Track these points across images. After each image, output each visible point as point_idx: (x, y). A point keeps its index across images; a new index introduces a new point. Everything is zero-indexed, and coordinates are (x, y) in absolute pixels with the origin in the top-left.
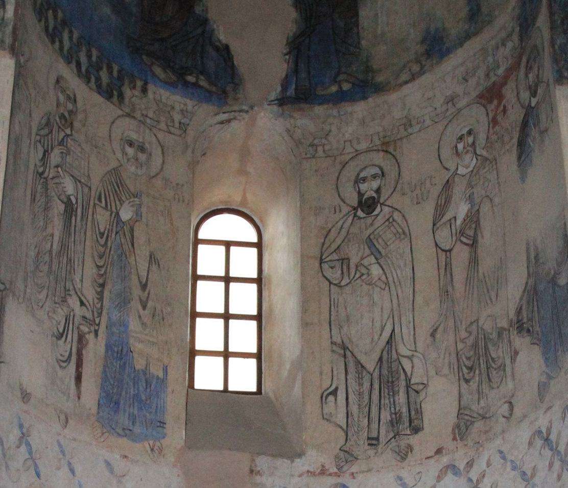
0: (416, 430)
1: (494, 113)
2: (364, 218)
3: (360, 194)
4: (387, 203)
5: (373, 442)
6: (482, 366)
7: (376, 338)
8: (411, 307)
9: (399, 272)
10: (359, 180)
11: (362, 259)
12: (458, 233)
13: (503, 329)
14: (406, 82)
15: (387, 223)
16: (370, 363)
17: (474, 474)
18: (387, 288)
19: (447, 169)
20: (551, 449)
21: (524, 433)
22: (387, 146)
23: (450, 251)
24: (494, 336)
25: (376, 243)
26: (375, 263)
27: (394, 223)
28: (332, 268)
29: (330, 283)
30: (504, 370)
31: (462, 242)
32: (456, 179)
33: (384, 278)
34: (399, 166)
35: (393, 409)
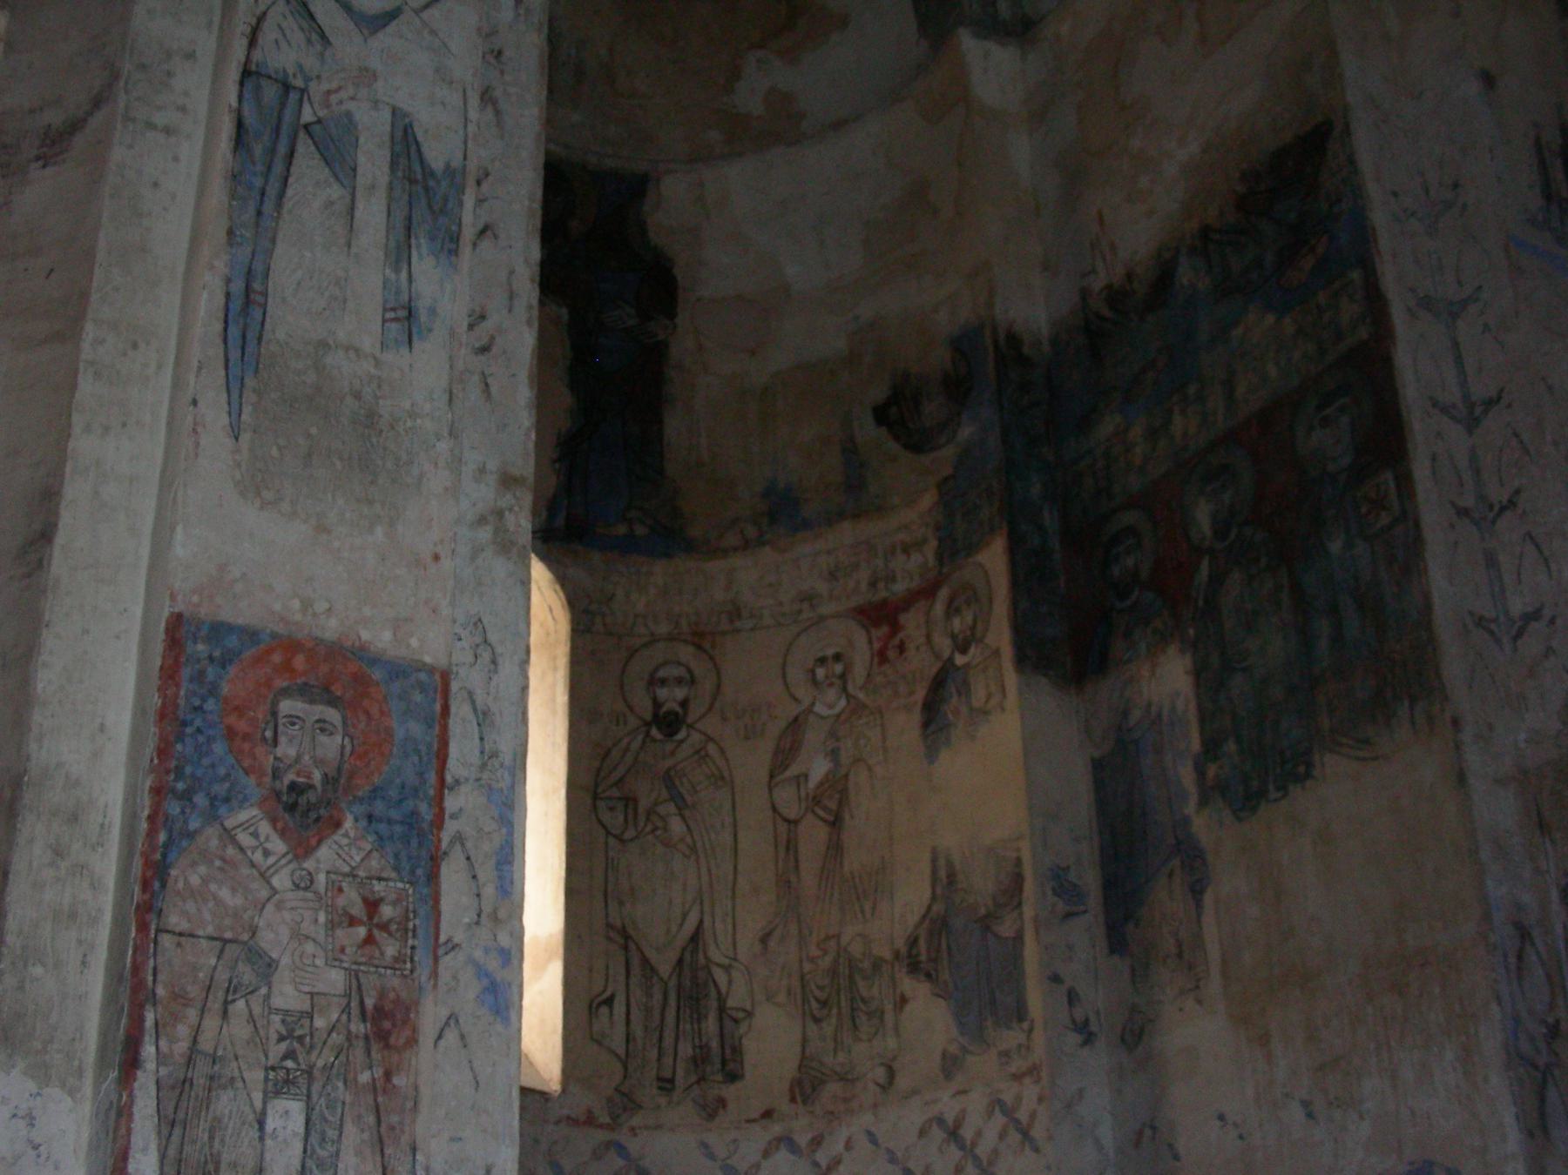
0: (733, 1077)
1: (882, 643)
2: (661, 741)
3: (657, 704)
4: (696, 726)
5: (666, 1084)
6: (843, 1004)
7: (674, 929)
8: (730, 894)
9: (713, 835)
10: (654, 681)
11: (656, 804)
12: (810, 799)
13: (882, 959)
14: (735, 549)
15: (696, 757)
16: (665, 968)
17: (822, 1157)
18: (693, 858)
19: (796, 700)
20: (962, 1147)
21: (913, 1116)
22: (701, 639)
23: (796, 822)
24: (866, 964)
25: (677, 783)
26: (676, 815)
27: (707, 759)
28: (611, 809)
29: (608, 833)
30: (882, 1020)
31: (813, 811)
32: (812, 718)
33: (689, 840)
34: (719, 674)
35: (697, 1040)
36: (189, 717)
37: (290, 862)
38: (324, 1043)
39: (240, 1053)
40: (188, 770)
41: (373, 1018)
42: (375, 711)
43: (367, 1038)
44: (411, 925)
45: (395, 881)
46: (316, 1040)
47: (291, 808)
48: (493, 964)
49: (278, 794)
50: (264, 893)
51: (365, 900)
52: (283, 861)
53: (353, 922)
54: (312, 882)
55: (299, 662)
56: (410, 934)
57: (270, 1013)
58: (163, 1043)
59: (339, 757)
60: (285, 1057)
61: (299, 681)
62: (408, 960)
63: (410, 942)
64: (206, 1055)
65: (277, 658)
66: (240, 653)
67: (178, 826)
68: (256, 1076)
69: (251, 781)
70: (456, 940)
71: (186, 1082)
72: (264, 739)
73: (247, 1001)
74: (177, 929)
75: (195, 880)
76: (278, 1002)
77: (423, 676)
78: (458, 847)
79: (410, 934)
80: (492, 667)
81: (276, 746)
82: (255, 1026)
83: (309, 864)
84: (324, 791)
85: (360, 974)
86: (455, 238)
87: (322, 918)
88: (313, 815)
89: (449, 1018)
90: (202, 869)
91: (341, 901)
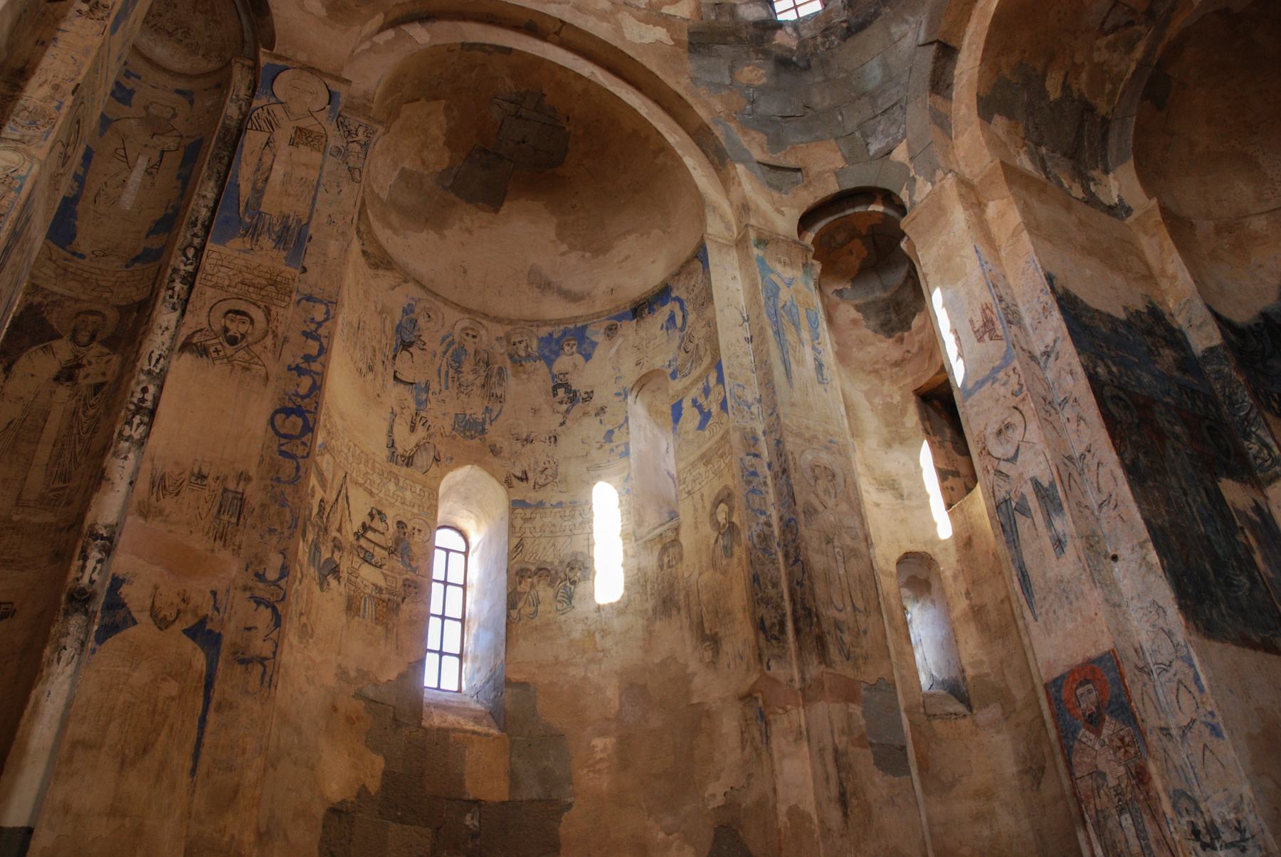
48: (1209, 719)
53: (1119, 748)
65: (1071, 679)
68: (1114, 811)
71: (1098, 821)
76: (1110, 785)
86: (1061, 505)
91: (1114, 744)
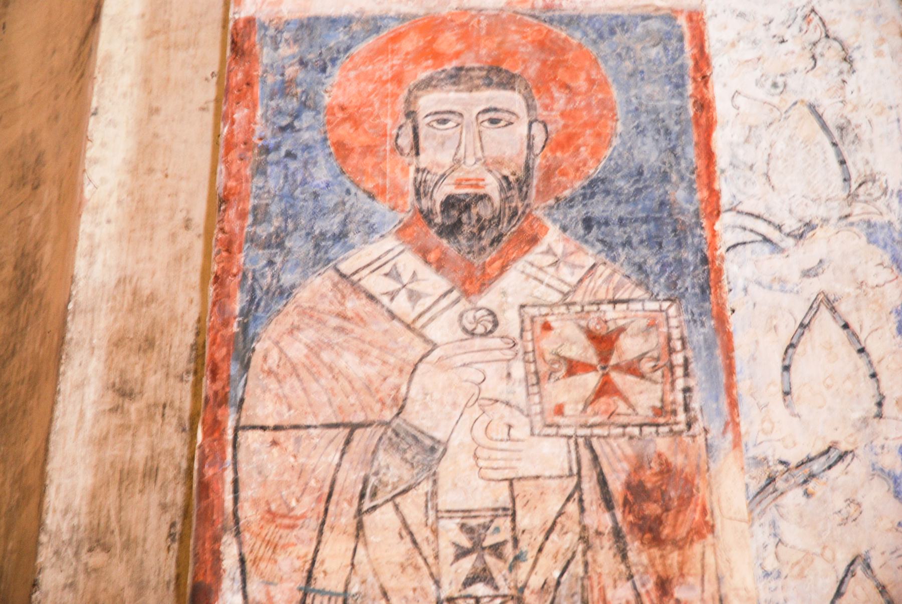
36: (272, 142)
37: (457, 301)
38: (540, 550)
39: (390, 584)
40: (274, 209)
41: (626, 502)
42: (581, 84)
43: (617, 534)
44: (678, 359)
45: (643, 301)
46: (523, 545)
47: (451, 230)
49: (427, 216)
50: (420, 348)
51: (593, 337)
52: (445, 302)
53: (573, 368)
54: (496, 324)
55: (448, 41)
56: (679, 372)
57: (438, 518)
58: (255, 588)
59: (525, 152)
60: (470, 581)
61: (449, 66)
62: (680, 410)
63: (680, 384)
64: (331, 594)
65: (409, 45)
66: (348, 49)
67: (265, 282)
69: (381, 206)
70: (843, 447)
72: (397, 148)
73: (397, 507)
74: (271, 423)
75: (296, 351)
77: (654, 25)
78: (825, 313)
79: (679, 372)
80: (845, 66)
81: (417, 154)
82: (414, 542)
83: (489, 299)
84: (505, 200)
85: (595, 442)
87: (518, 370)
88: (487, 237)
89: (852, 563)
90: (308, 335)
91: (548, 344)
